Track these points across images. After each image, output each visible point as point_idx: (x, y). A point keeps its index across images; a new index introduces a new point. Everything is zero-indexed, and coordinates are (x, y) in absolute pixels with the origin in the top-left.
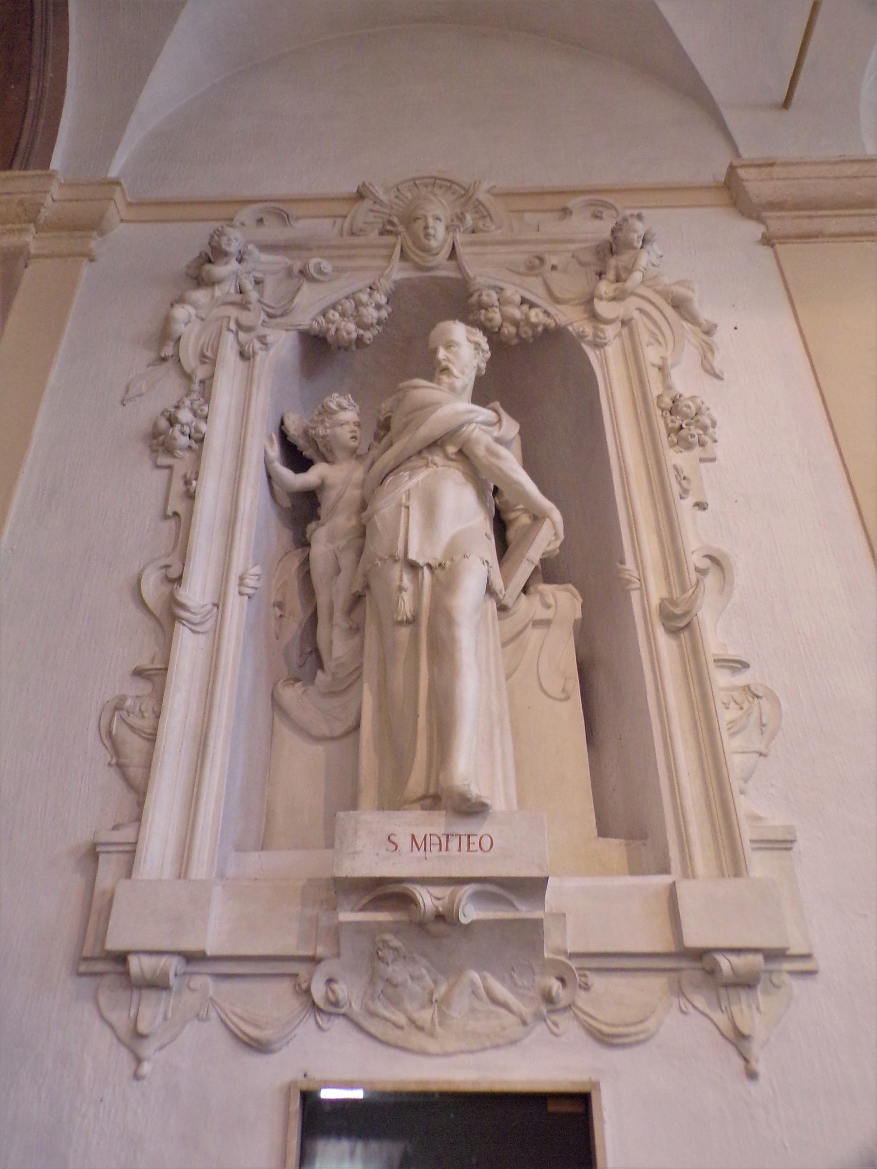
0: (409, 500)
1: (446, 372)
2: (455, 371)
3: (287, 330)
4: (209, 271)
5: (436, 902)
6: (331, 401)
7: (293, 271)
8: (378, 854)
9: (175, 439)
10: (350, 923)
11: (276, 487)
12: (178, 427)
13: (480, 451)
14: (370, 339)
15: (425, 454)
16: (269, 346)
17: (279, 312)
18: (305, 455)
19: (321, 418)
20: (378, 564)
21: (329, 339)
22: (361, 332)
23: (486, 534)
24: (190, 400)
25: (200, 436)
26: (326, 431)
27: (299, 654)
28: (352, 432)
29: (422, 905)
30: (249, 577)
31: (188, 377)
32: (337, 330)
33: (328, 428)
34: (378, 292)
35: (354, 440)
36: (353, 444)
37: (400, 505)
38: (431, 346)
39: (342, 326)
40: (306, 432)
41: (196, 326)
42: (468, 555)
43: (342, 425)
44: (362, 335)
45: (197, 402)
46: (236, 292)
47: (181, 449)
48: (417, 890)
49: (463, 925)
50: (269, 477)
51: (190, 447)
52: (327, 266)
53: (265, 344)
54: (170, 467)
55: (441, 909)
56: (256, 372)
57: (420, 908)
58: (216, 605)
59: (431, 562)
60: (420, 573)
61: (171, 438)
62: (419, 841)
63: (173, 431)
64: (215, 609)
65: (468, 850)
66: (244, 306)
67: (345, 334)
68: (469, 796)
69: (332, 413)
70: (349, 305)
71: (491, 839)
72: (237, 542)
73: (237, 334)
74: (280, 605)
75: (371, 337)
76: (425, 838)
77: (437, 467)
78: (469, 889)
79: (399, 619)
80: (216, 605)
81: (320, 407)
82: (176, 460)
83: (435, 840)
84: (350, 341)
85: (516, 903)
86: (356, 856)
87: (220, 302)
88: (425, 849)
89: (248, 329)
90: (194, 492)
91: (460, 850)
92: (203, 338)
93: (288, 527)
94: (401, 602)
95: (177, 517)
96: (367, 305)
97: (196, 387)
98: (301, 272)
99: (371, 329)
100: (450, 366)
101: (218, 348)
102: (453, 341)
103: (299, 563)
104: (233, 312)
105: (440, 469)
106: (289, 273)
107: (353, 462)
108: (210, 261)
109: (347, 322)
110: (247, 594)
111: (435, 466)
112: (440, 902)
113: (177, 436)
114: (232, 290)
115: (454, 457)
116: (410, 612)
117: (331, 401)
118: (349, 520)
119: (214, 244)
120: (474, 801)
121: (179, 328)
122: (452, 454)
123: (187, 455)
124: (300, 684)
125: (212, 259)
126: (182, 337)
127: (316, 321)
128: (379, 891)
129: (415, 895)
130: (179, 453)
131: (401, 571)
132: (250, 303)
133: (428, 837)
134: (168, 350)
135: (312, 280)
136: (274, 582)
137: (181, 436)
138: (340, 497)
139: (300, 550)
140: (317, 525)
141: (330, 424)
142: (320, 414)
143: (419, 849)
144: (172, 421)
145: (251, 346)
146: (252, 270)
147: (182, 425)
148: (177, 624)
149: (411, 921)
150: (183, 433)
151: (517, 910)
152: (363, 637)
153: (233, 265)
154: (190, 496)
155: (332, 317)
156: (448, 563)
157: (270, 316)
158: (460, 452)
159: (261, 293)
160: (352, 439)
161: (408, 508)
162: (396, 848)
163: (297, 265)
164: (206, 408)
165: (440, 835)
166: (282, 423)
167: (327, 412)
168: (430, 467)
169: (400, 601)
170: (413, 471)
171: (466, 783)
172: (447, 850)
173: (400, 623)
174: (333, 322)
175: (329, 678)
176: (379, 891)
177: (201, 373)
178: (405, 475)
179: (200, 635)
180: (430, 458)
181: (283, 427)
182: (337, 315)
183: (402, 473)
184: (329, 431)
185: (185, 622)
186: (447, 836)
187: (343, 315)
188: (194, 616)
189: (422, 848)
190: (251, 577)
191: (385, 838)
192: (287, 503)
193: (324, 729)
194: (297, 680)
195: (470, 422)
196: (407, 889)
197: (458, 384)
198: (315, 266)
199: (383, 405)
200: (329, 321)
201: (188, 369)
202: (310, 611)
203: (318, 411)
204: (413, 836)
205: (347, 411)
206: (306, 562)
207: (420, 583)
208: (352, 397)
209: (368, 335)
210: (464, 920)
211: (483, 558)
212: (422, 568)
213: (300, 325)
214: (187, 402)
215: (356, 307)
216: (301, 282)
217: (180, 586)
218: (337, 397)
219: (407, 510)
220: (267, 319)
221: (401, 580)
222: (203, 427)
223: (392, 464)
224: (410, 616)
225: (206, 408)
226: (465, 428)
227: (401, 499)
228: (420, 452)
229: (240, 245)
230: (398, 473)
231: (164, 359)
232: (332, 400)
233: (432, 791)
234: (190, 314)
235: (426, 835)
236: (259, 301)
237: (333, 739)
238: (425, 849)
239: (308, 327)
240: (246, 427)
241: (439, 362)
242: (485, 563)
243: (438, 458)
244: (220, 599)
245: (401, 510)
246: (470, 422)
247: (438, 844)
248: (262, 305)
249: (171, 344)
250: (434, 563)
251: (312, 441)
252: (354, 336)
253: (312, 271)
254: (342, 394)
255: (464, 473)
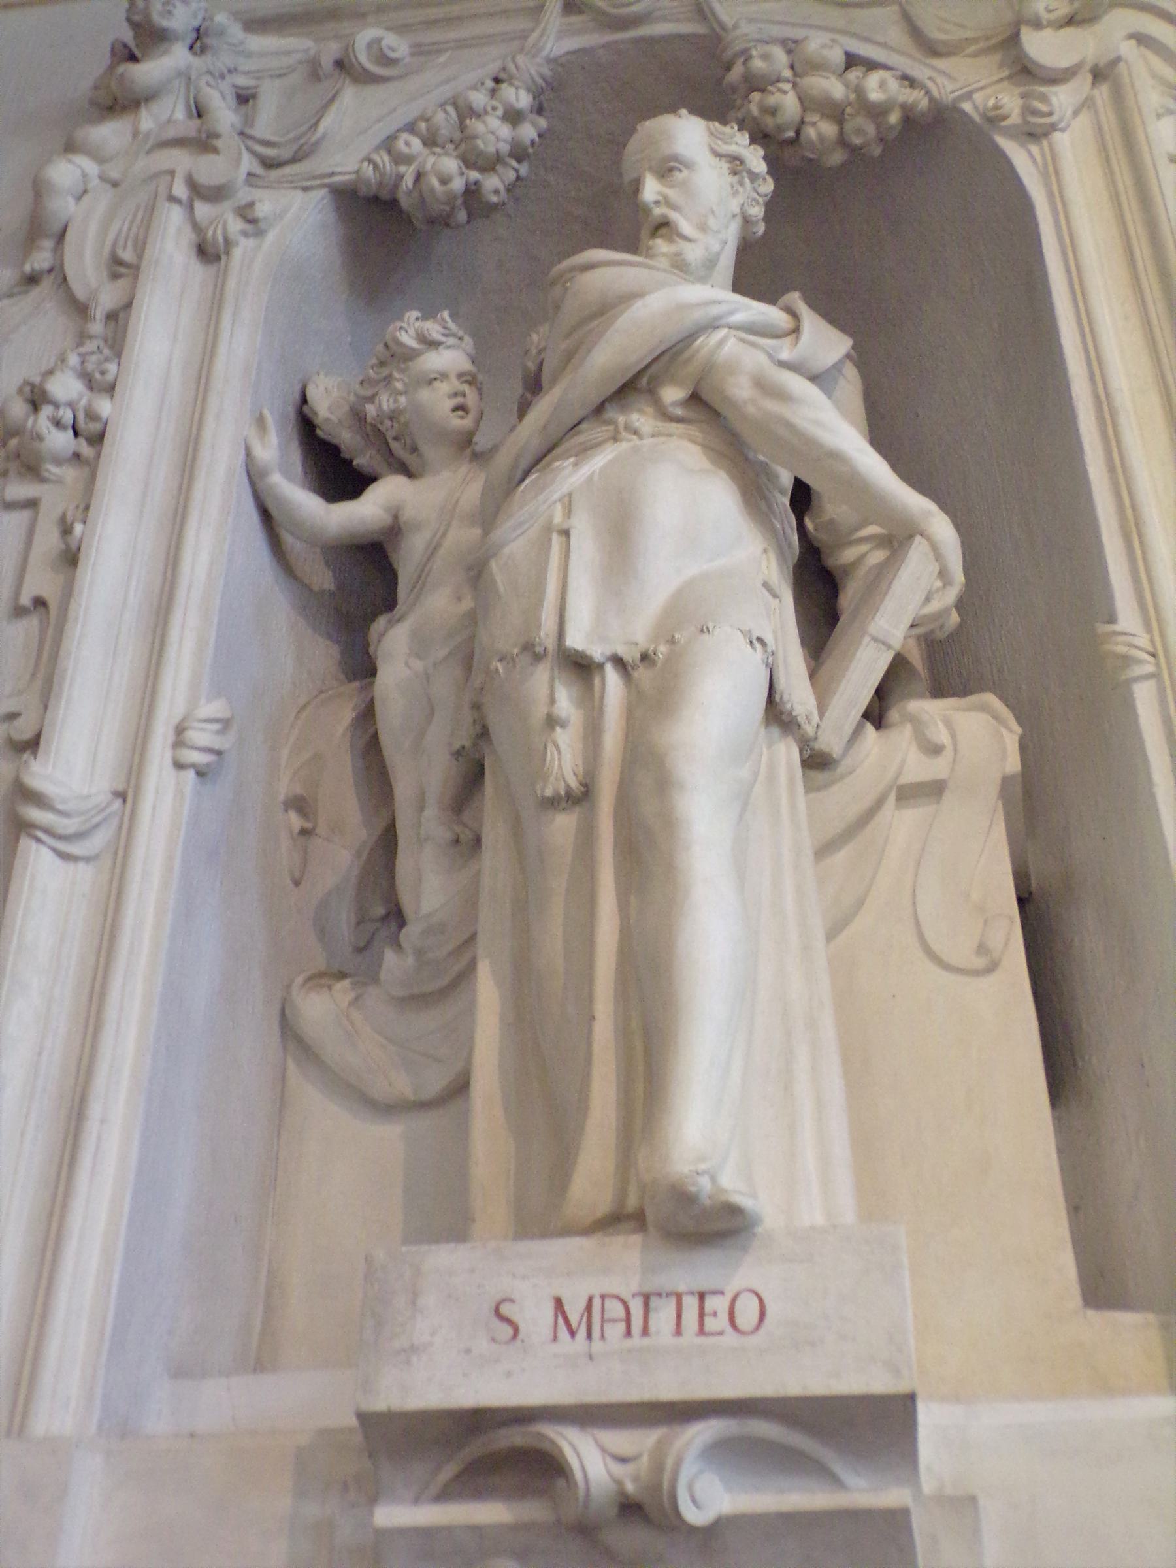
0: (569, 518)
1: (663, 231)
2: (685, 226)
3: (305, 189)
4: (122, 75)
5: (618, 1469)
6: (401, 328)
7: (320, 64)
8: (468, 1351)
9: (40, 438)
10: (403, 1532)
11: (288, 539)
12: (47, 411)
13: (741, 390)
14: (496, 192)
15: (611, 413)
16: (262, 225)
17: (286, 153)
18: (358, 465)
19: (385, 372)
20: (497, 670)
21: (405, 202)
22: (474, 175)
23: (766, 585)
24: (80, 355)
25: (95, 427)
26: (396, 401)
27: (353, 920)
28: (456, 395)
29: (578, 1475)
30: (197, 725)
31: (80, 309)
32: (419, 177)
33: (401, 394)
34: (511, 84)
35: (460, 413)
36: (458, 422)
37: (548, 529)
38: (627, 178)
39: (428, 167)
40: (358, 417)
41: (102, 200)
42: (711, 625)
43: (430, 382)
44: (476, 183)
45: (94, 358)
46: (190, 116)
47: (58, 462)
48: (566, 1438)
49: (692, 1530)
50: (266, 515)
51: (77, 456)
52: (397, 45)
53: (252, 221)
54: (32, 504)
55: (630, 1487)
56: (231, 284)
57: (576, 1484)
58: (122, 796)
59: (621, 651)
60: (597, 681)
61: (32, 435)
62: (575, 1313)
63: (35, 421)
64: (118, 803)
65: (702, 1331)
66: (204, 143)
67: (435, 182)
68: (693, 1189)
69: (410, 356)
70: (445, 121)
71: (761, 1300)
72: (171, 653)
73: (191, 208)
74: (300, 804)
75: (501, 188)
76: (589, 1307)
77: (641, 437)
78: (701, 1433)
79: (549, 792)
80: (122, 796)
81: (380, 347)
82: (46, 487)
83: (615, 1309)
84: (451, 198)
85: (838, 1468)
86: (414, 1359)
87: (150, 143)
88: (589, 1335)
89: (216, 194)
90: (79, 549)
91: (678, 1331)
92: (115, 227)
93: (329, 636)
94: (552, 754)
95: (42, 609)
96: (486, 112)
97: (97, 327)
98: (340, 64)
99: (499, 167)
100: (674, 216)
101: (145, 243)
102: (675, 158)
103: (354, 715)
104: (181, 161)
105: (648, 442)
106: (314, 72)
107: (464, 468)
108: (133, 58)
109: (439, 155)
110: (193, 766)
111: (635, 437)
112: (630, 1468)
113: (46, 431)
114: (180, 115)
115: (679, 412)
116: (575, 774)
117: (401, 328)
118: (459, 599)
119: (137, 18)
120: (708, 1202)
121: (63, 206)
122: (674, 404)
123: (70, 474)
124: (346, 983)
125: (138, 54)
126: (70, 224)
127: (370, 161)
128: (476, 1448)
129: (561, 1451)
130: (52, 469)
131: (552, 679)
132: (217, 136)
133: (597, 1303)
134: (41, 259)
135: (365, 78)
136: (285, 752)
137: (54, 430)
138: (433, 550)
139: (356, 684)
140: (389, 621)
141: (405, 384)
142: (382, 364)
143: (573, 1333)
144: (36, 399)
145: (220, 226)
146: (230, 71)
147: (57, 406)
148: (25, 843)
149: (559, 1521)
150: (58, 424)
151: (837, 1482)
152: (37, 513)
153: (177, 57)
154: (71, 559)
155: (405, 149)
156: (663, 649)
157: (270, 164)
158: (695, 399)
159: (249, 121)
160: (455, 413)
161: (566, 533)
162: (516, 1331)
163: (331, 51)
164: (112, 368)
165: (626, 1295)
166: (304, 400)
167: (397, 356)
168: (621, 441)
169: (549, 752)
170: (586, 450)
171: (702, 1167)
172: (645, 1331)
173: (553, 803)
174: (407, 160)
175: (410, 960)
176: (476, 1448)
177: (107, 298)
178: (565, 465)
179: (81, 865)
180: (621, 419)
181: (305, 408)
182: (416, 143)
183: (557, 464)
184: (403, 400)
185: (40, 834)
186: (647, 1299)
187: (430, 141)
188: (65, 821)
189: (582, 1333)
190: (204, 725)
191: (487, 1308)
192: (323, 579)
193: (401, 1085)
194: (342, 975)
195: (713, 325)
196: (540, 1436)
197: (694, 254)
198: (369, 46)
199: (535, 337)
200: (400, 159)
201: (80, 293)
202: (381, 825)
203: (378, 359)
204: (559, 1303)
205: (441, 348)
206: (368, 714)
207: (597, 703)
208: (451, 316)
209: (492, 184)
210: (693, 1516)
211: (750, 631)
212: (601, 666)
213: (333, 174)
214: (73, 360)
215: (461, 119)
216: (338, 86)
217: (35, 758)
218: (417, 319)
219: (564, 539)
220: (259, 170)
221: (552, 701)
222: (104, 407)
223: (536, 445)
224: (573, 783)
225: (112, 368)
226: (701, 339)
227: (551, 518)
228: (599, 409)
229: (195, 17)
230: (549, 464)
231: (32, 280)
232: (405, 325)
233: (632, 1203)
234: (85, 175)
235: (590, 1300)
236: (242, 133)
237: (423, 1106)
238: (589, 1335)
239: (353, 177)
240: (204, 400)
241: (647, 211)
242: (758, 645)
243: (642, 419)
244: (128, 781)
245: (550, 540)
246: (713, 325)
247: (621, 1320)
248: (250, 143)
249: (48, 244)
250: (629, 654)
251: (374, 434)
252: (458, 185)
253: (363, 58)
254: (429, 314)
255: (706, 447)
